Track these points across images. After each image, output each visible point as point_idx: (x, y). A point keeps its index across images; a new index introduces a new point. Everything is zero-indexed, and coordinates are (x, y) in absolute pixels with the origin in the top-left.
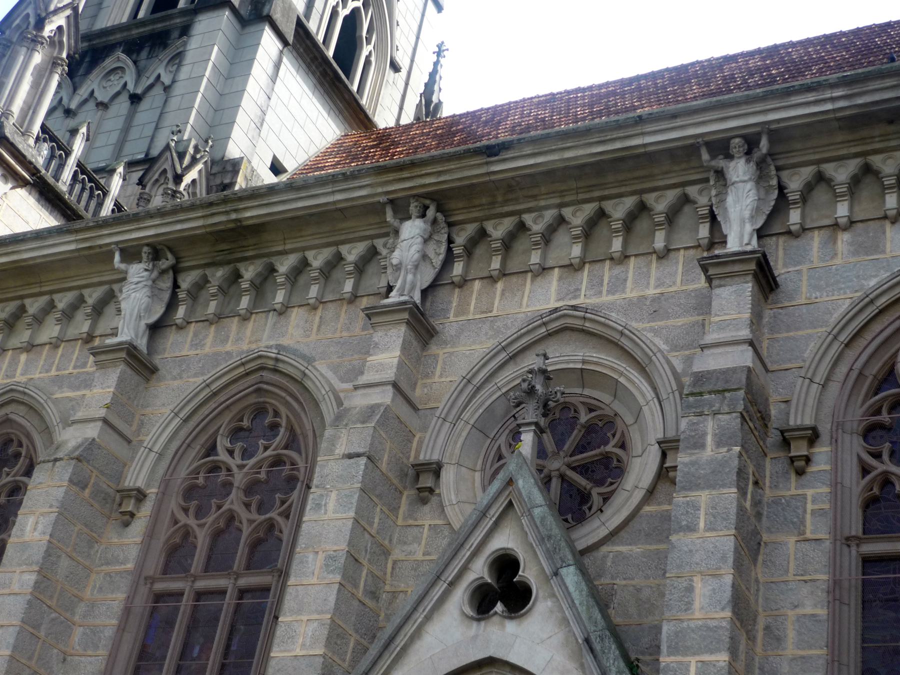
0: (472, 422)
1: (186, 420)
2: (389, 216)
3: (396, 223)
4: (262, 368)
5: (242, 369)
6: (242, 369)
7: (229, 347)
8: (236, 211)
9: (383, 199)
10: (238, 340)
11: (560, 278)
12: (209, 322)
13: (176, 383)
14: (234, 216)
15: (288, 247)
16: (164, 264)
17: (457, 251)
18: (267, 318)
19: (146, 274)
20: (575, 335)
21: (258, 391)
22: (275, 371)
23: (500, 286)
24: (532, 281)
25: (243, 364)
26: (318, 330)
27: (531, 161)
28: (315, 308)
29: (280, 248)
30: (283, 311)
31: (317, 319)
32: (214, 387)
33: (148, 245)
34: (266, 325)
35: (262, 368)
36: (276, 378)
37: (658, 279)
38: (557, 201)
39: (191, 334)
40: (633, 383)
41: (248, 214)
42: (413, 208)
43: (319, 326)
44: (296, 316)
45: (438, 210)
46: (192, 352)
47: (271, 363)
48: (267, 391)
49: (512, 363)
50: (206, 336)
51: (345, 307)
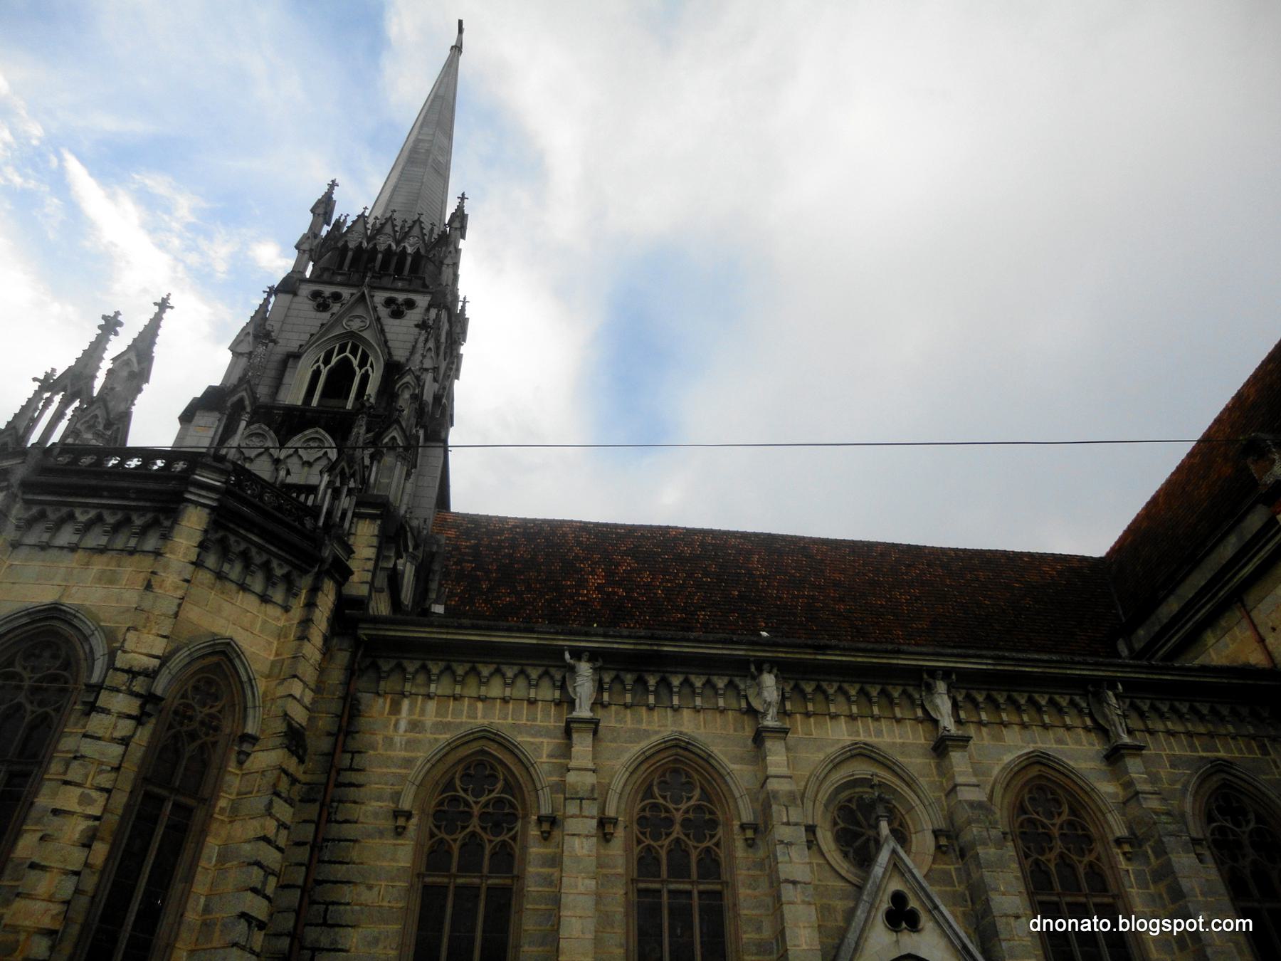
0: (823, 802)
1: (632, 773)
2: (753, 669)
3: (756, 673)
4: (676, 746)
5: (663, 745)
6: (663, 745)
7: (644, 726)
8: (657, 645)
9: (752, 659)
10: (649, 723)
11: (846, 722)
12: (626, 706)
13: (613, 745)
14: (655, 648)
15: (678, 670)
16: (598, 664)
17: (787, 695)
18: (666, 712)
19: (591, 671)
20: (865, 759)
21: (676, 759)
22: (686, 749)
23: (812, 720)
24: (831, 721)
25: (665, 742)
26: (705, 727)
27: (839, 658)
28: (698, 711)
29: (673, 670)
30: (676, 710)
31: (702, 719)
32: (647, 754)
33: (588, 651)
34: (667, 715)
35: (676, 746)
36: (686, 753)
37: (900, 734)
38: (841, 679)
39: (613, 713)
40: (905, 792)
41: (666, 649)
42: (766, 666)
43: (705, 723)
44: (686, 713)
45: (778, 670)
46: (618, 725)
47: (683, 744)
48: (681, 761)
49: (834, 770)
50: (625, 716)
51: (718, 715)
